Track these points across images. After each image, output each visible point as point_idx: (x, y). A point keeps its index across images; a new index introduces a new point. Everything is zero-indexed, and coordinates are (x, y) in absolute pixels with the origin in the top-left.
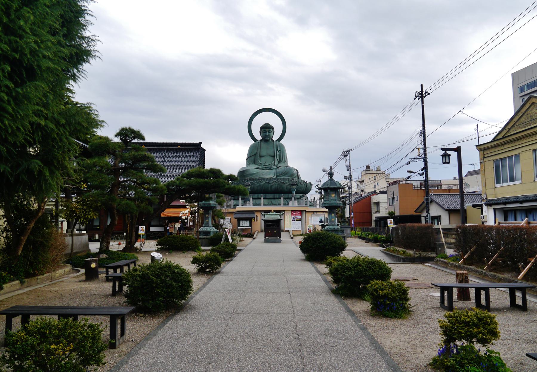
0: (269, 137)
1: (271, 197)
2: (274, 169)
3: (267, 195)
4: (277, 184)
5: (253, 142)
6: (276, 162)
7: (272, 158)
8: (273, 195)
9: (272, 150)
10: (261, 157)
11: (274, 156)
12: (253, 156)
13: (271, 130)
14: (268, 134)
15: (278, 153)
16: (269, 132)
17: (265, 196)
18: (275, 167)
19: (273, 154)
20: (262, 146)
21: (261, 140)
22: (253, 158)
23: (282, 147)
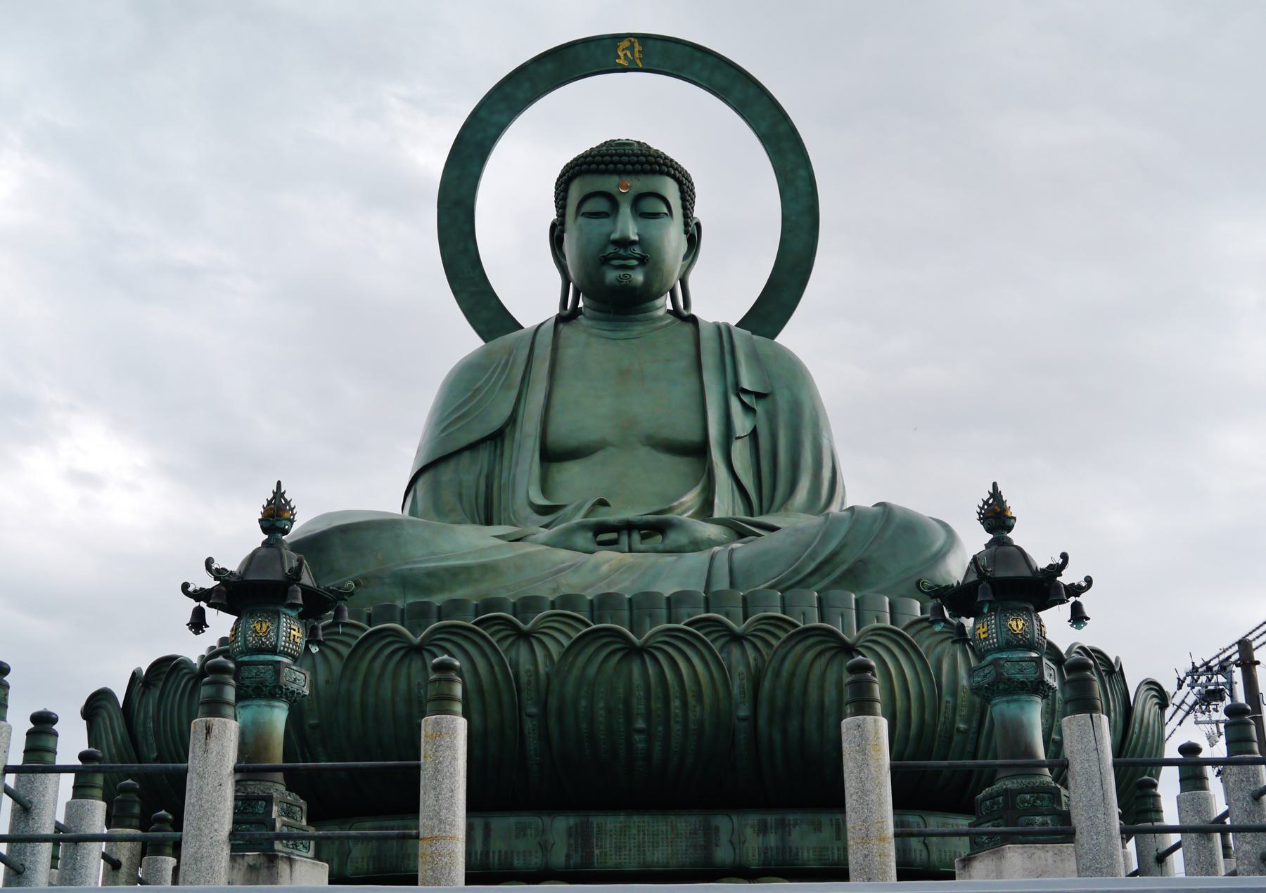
0: (647, 257)
1: (659, 856)
2: (697, 545)
3: (610, 823)
4: (739, 661)
5: (471, 342)
6: (726, 503)
7: (683, 465)
8: (685, 824)
9: (680, 393)
10: (551, 455)
11: (699, 451)
12: (469, 455)
13: (671, 190)
14: (629, 227)
15: (742, 424)
16: (647, 207)
17: (582, 837)
18: (710, 531)
19: (686, 431)
20: (569, 354)
21: (566, 317)
22: (469, 472)
23: (793, 371)
